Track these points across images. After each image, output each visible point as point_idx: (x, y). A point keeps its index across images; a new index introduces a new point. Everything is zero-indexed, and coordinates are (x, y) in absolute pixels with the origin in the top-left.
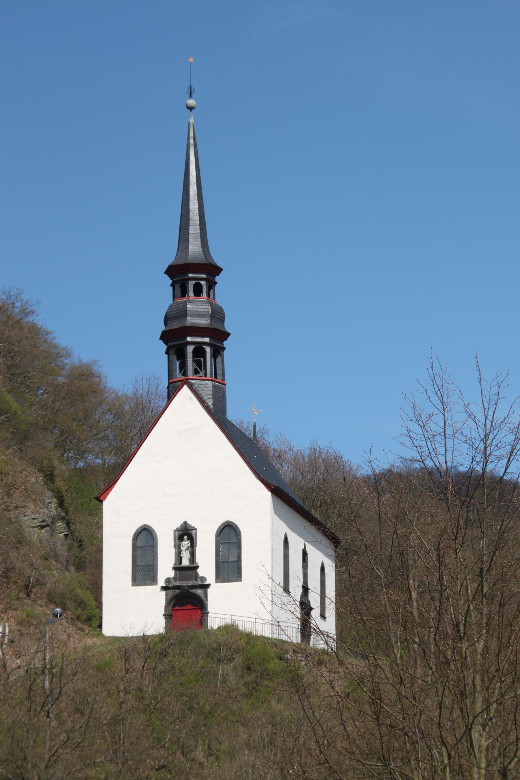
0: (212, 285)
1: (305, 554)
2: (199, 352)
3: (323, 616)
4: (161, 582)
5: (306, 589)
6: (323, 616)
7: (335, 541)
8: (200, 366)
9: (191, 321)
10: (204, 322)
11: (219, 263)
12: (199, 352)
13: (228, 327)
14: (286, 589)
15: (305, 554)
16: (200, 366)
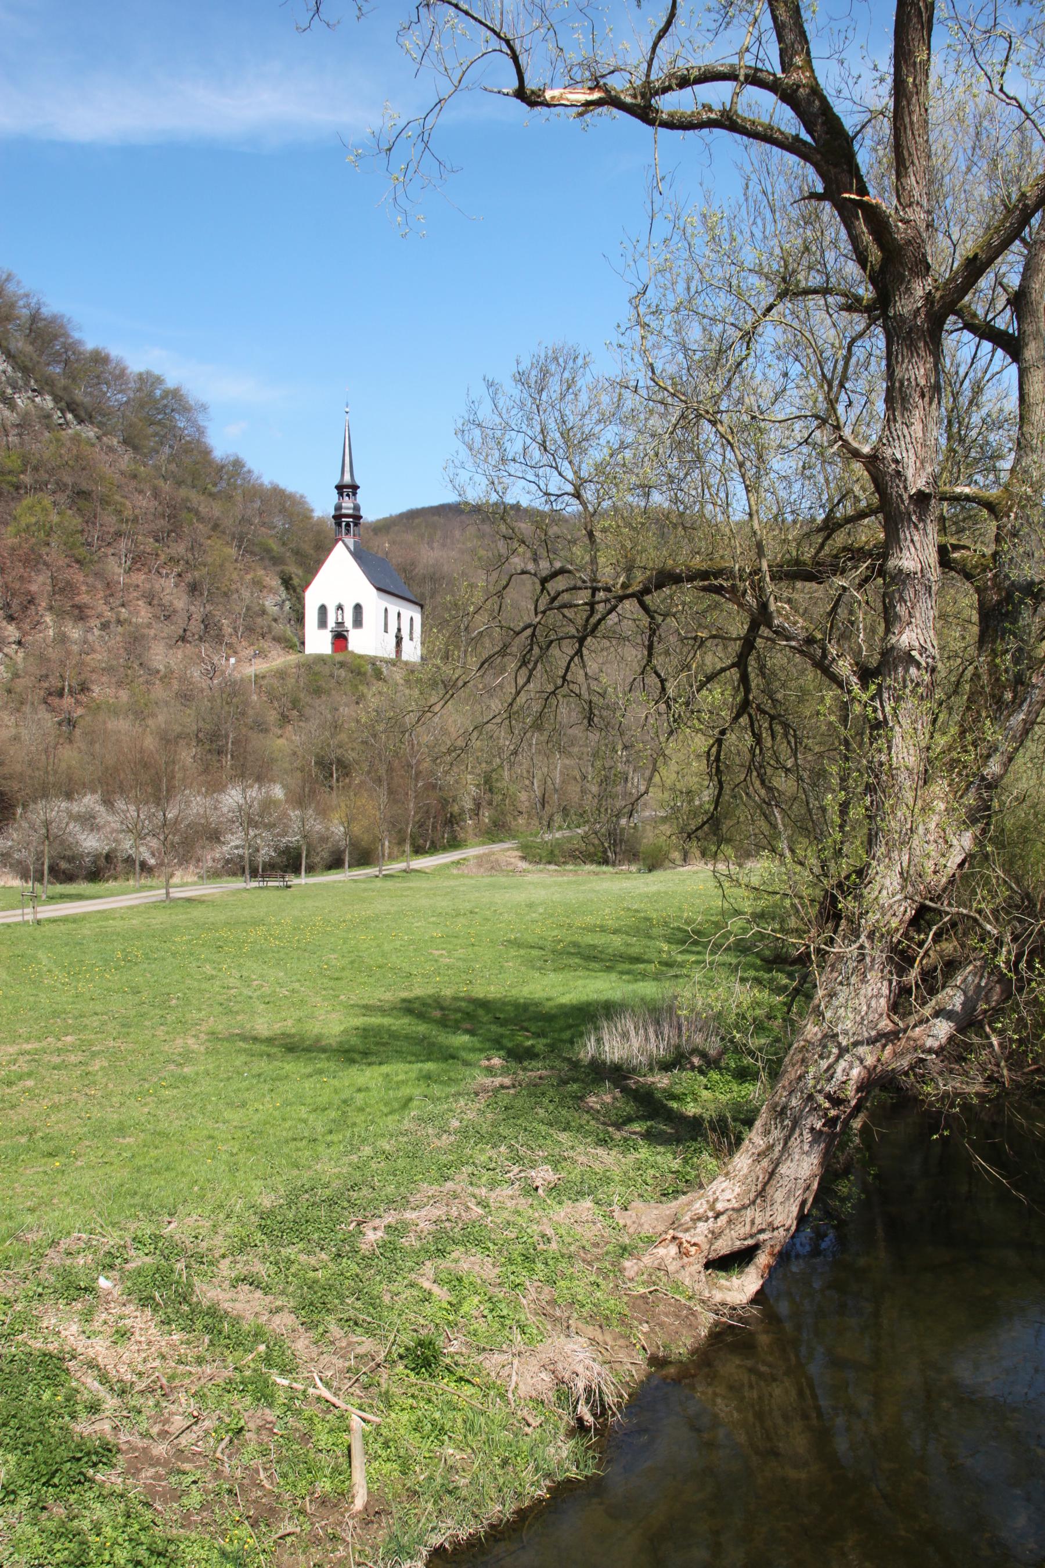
0: (355, 494)
1: (399, 614)
2: (348, 525)
3: (411, 639)
4: (330, 628)
5: (399, 630)
6: (411, 639)
7: (422, 606)
8: (348, 531)
9: (344, 511)
10: (350, 512)
11: (358, 482)
12: (348, 525)
13: (362, 513)
14: (386, 631)
15: (399, 614)
16: (348, 531)
